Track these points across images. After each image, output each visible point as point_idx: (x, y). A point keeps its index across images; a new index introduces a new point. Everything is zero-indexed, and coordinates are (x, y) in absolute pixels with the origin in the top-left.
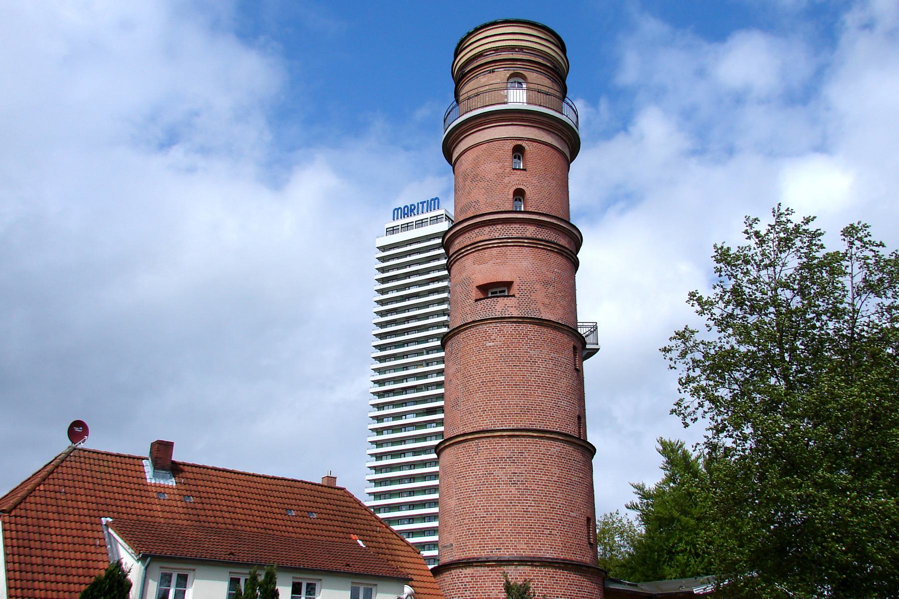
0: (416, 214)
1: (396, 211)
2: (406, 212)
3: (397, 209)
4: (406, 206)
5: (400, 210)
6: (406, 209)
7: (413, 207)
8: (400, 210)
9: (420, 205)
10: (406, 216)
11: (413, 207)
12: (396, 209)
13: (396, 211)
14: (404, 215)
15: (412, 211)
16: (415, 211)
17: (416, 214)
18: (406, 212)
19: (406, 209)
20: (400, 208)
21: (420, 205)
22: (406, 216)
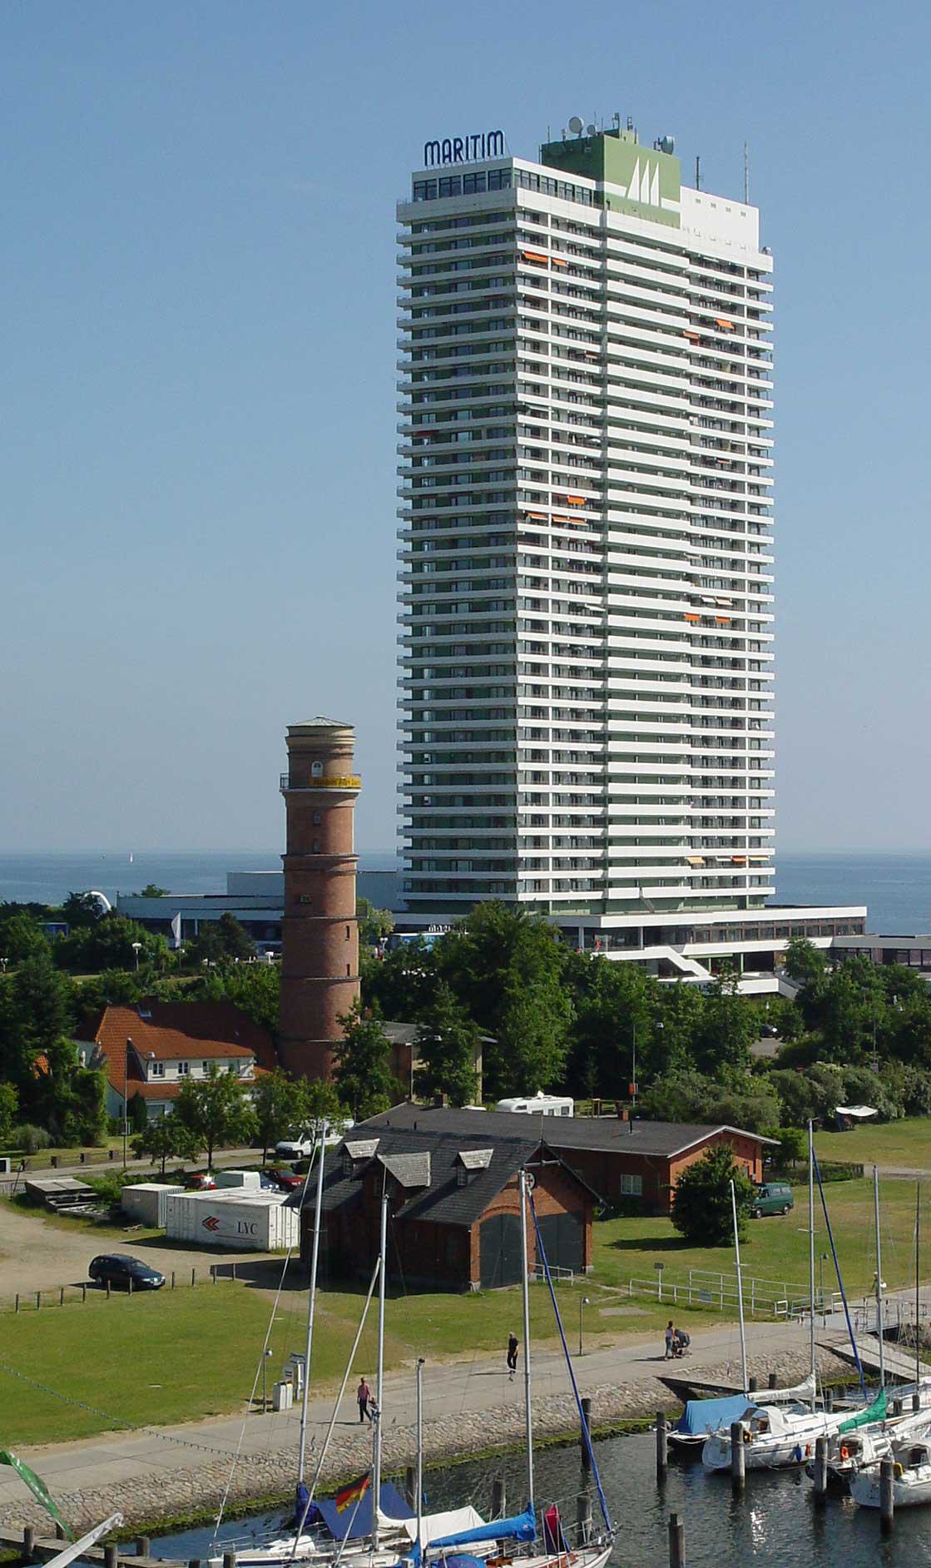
0: (464, 158)
1: (429, 148)
2: (446, 153)
3: (432, 145)
4: (448, 141)
5: (436, 147)
6: (447, 145)
7: (458, 144)
8: (436, 147)
9: (471, 141)
10: (447, 160)
11: (458, 144)
12: (429, 144)
13: (429, 148)
14: (444, 157)
15: (457, 151)
16: (463, 153)
17: (464, 158)
18: (446, 153)
19: (447, 145)
20: (436, 143)
21: (471, 141)
22: (447, 160)
